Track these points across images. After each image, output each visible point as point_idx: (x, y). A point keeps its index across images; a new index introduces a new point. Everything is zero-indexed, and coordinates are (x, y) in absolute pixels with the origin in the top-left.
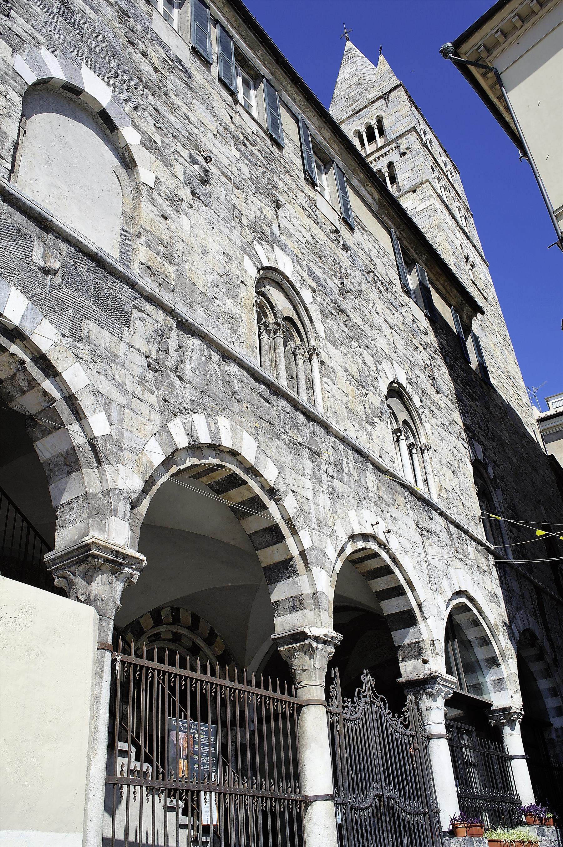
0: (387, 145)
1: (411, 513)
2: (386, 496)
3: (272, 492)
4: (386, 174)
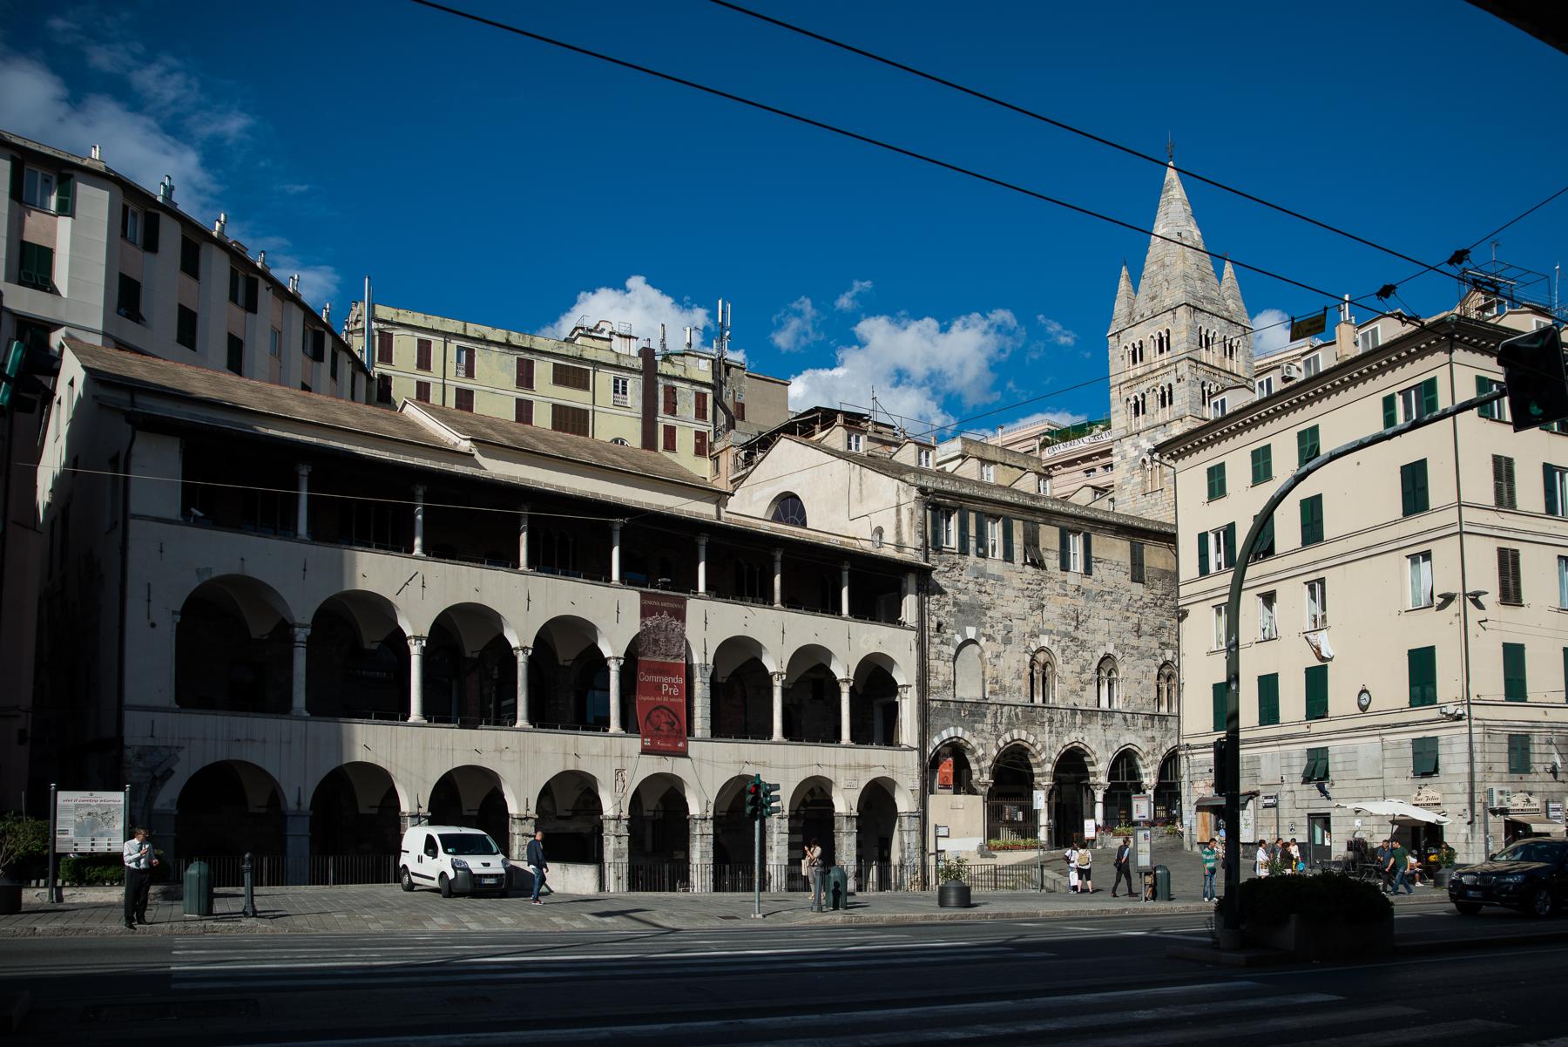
1: (1100, 722)
2: (1084, 722)
4: (1167, 394)
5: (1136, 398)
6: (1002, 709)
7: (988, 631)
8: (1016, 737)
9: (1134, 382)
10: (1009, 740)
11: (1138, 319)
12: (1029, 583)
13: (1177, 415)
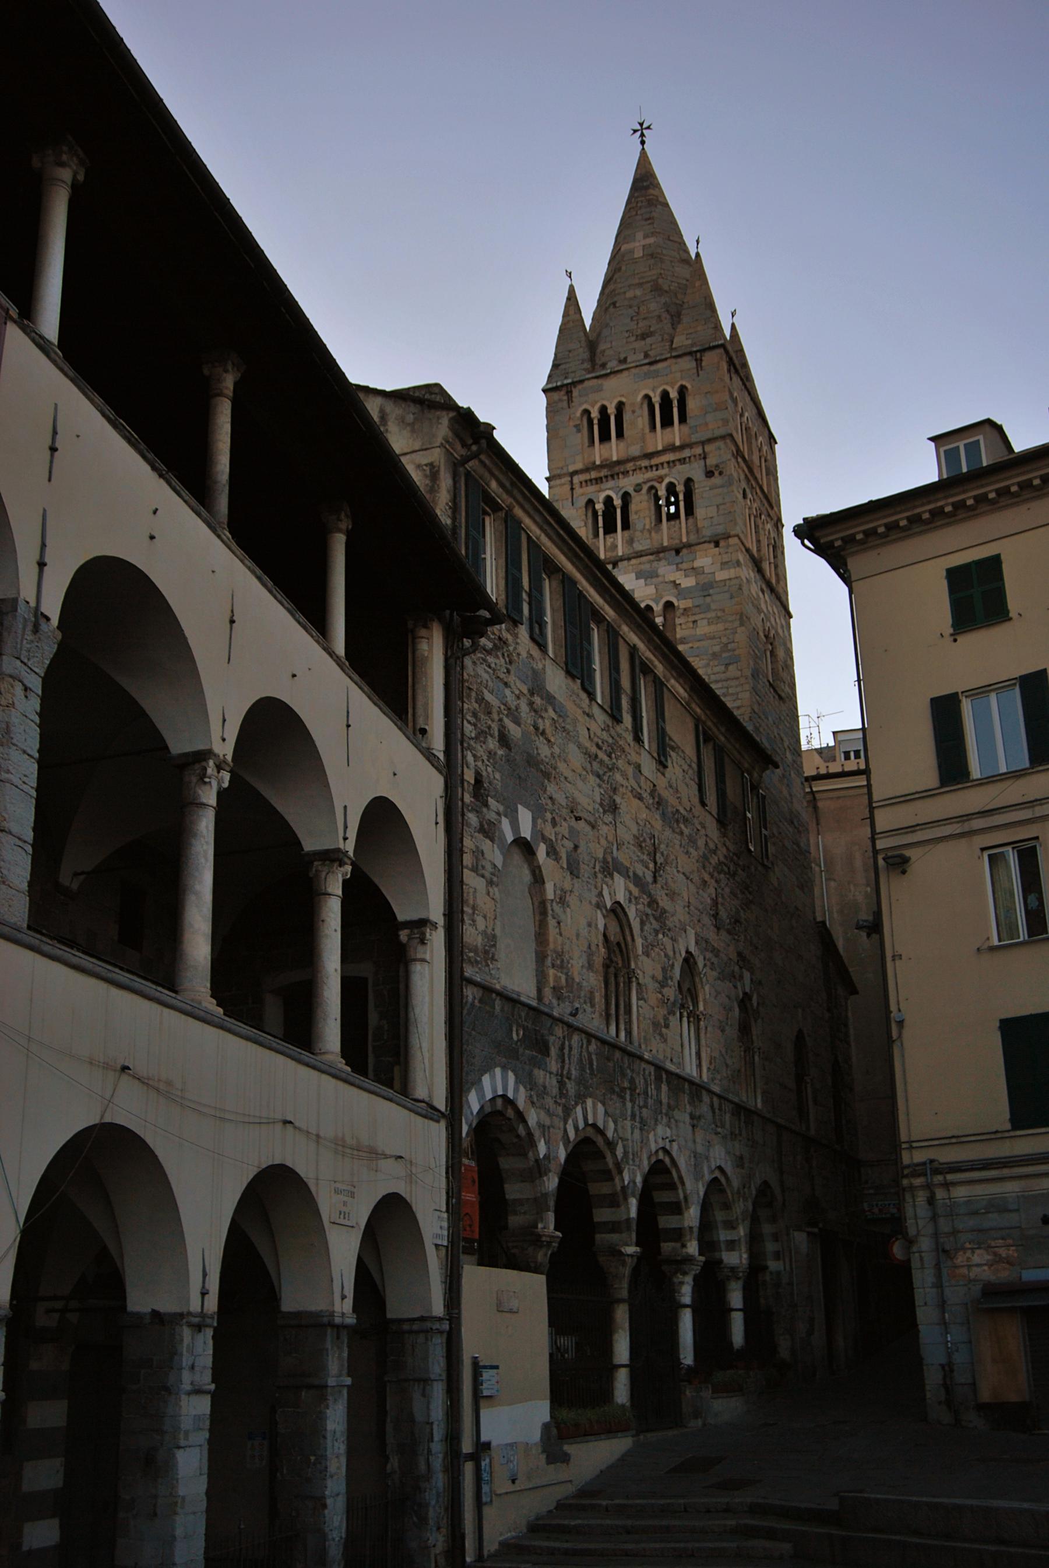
0: (690, 446)
1: (688, 1108)
2: (672, 1103)
3: (611, 1145)
5: (608, 500)
6: (570, 1040)
7: (549, 832)
8: (590, 1122)
9: (604, 472)
10: (581, 1125)
11: (613, 365)
12: (598, 746)
13: (707, 533)
